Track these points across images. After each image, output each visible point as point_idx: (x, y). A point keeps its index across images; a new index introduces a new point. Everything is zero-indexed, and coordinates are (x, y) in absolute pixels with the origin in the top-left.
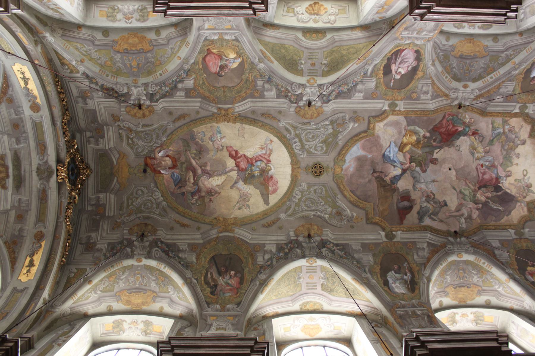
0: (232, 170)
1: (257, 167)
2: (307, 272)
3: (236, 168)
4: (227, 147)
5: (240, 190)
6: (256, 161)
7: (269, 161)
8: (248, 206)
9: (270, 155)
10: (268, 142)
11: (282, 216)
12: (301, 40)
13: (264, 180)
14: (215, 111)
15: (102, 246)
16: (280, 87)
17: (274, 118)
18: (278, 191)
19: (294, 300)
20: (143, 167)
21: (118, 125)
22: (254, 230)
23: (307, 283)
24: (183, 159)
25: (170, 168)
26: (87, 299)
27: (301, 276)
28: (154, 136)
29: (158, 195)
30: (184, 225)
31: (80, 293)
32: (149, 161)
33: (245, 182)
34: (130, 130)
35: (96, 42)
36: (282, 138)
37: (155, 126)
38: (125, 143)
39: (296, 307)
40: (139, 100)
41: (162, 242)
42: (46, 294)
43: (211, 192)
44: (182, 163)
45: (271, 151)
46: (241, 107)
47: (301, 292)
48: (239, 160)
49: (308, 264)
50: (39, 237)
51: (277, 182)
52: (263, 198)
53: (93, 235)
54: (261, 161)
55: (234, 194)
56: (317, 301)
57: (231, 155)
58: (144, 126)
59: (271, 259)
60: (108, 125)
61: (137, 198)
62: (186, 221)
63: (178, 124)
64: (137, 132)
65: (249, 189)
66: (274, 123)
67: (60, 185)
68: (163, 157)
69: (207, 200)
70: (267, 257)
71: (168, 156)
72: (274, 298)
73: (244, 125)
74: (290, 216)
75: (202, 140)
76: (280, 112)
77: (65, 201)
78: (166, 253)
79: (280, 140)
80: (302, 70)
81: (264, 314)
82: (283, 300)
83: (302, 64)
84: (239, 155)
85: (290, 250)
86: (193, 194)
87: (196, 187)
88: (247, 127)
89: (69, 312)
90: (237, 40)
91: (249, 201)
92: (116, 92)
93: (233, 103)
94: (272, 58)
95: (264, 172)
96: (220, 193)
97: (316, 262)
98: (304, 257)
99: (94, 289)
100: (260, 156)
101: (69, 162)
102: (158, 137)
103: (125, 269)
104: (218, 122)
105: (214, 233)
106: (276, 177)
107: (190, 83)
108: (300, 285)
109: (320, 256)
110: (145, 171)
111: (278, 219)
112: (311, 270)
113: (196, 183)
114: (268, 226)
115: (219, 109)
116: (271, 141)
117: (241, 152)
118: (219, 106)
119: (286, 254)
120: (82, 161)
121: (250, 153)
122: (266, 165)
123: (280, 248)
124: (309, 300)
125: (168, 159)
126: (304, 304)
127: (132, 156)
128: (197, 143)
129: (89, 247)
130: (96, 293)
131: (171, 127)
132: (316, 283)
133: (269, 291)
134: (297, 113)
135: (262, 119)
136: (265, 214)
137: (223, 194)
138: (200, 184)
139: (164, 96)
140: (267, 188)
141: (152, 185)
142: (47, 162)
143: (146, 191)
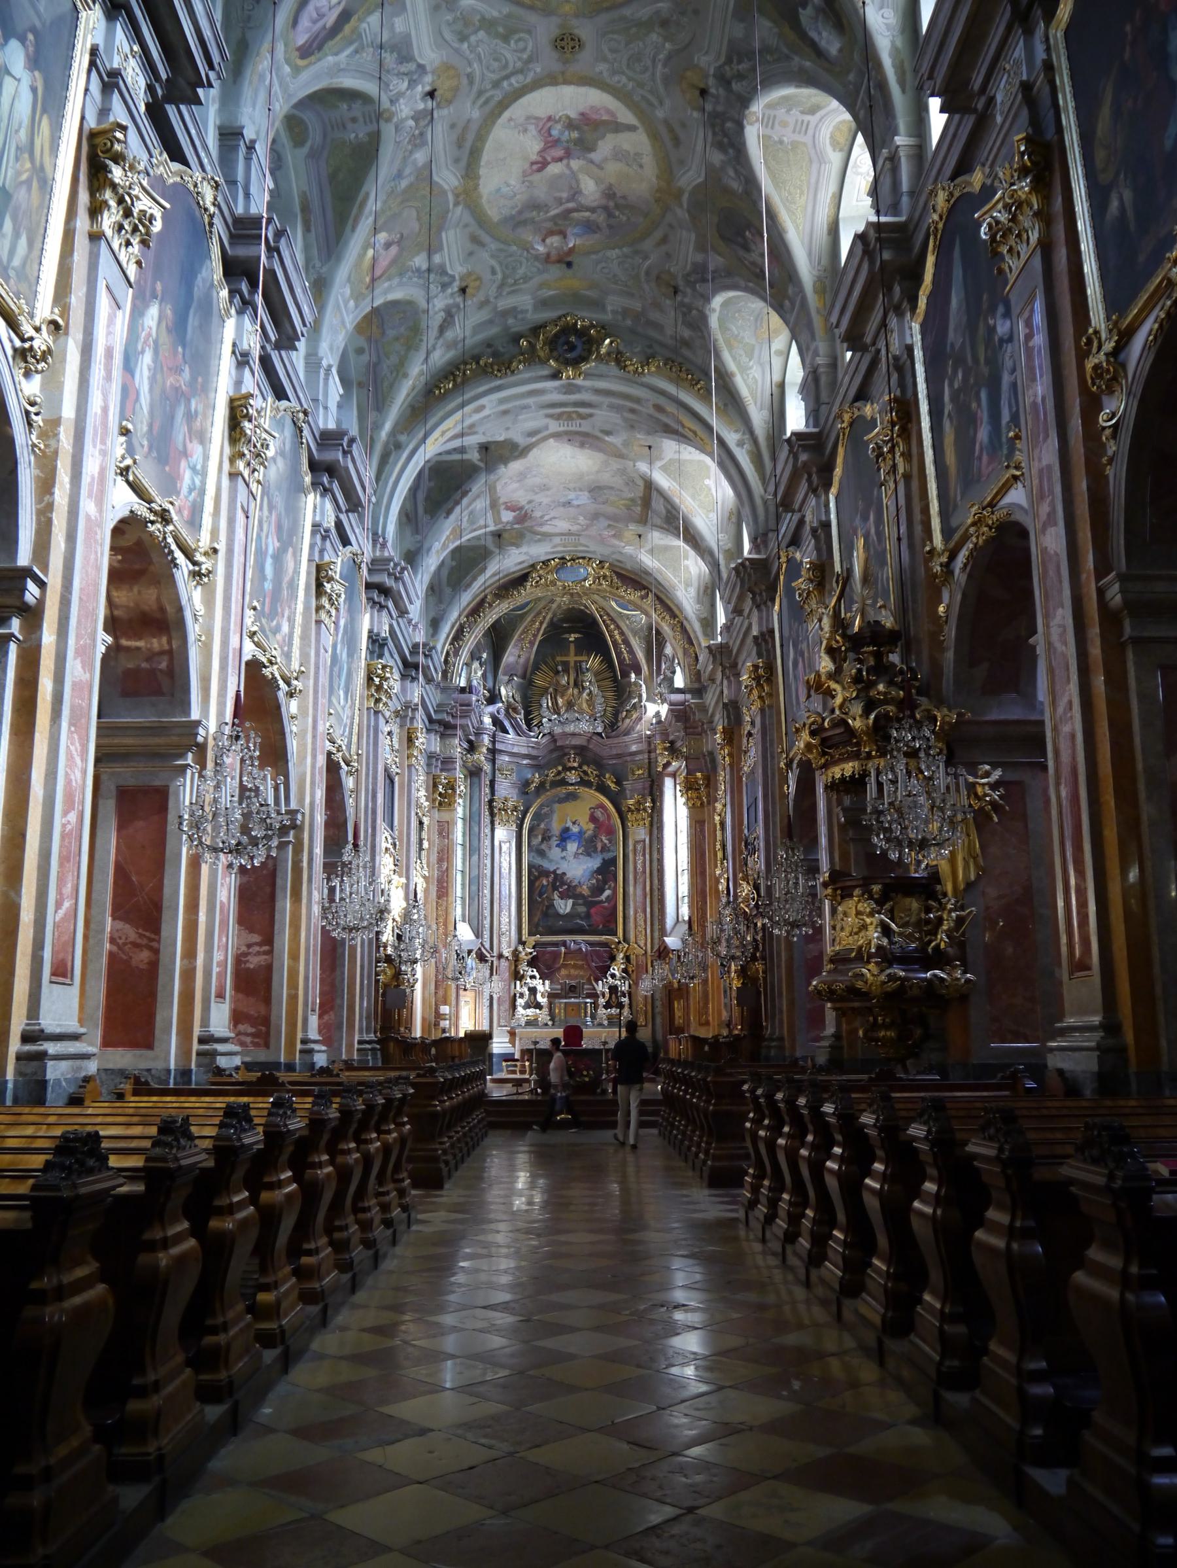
0: (568, 166)
1: (562, 133)
2: (772, 128)
3: (565, 162)
4: (524, 176)
5: (606, 160)
6: (550, 135)
7: (550, 118)
8: (636, 154)
9: (537, 118)
10: (512, 123)
11: (660, 114)
12: (311, 148)
13: (587, 125)
14: (460, 208)
15: (686, 333)
16: (407, 154)
17: (465, 128)
18: (611, 107)
19: (822, 160)
20: (564, 266)
21: (496, 298)
22: (682, 162)
23: (794, 132)
24: (549, 225)
25: (565, 237)
26: (756, 381)
27: (776, 139)
28: (510, 259)
29: (613, 253)
30: (664, 240)
31: (744, 391)
32: (554, 257)
33: (591, 149)
34: (502, 286)
35: (374, 359)
36: (504, 105)
37: (493, 262)
38: (523, 286)
39: (836, 158)
40: (452, 294)
41: (688, 275)
42: (732, 438)
43: (609, 193)
44: (556, 224)
45: (528, 118)
46: (448, 178)
47: (810, 143)
48: (549, 159)
49: (756, 125)
50: (659, 408)
51: (592, 107)
52: (622, 131)
53: (669, 331)
54: (550, 129)
55: (613, 168)
56: (833, 124)
57: (540, 170)
58: (494, 272)
59: (736, 171)
60: (496, 307)
61: (615, 276)
62: (658, 234)
63: (486, 238)
64: (505, 277)
65: (605, 147)
66: (474, 127)
67: (588, 376)
68: (545, 246)
69: (622, 201)
70: (731, 173)
71: (543, 240)
72: (804, 198)
73: (482, 163)
74: (661, 103)
75: (513, 208)
76: (453, 126)
77: (612, 369)
78: (704, 280)
79: (507, 107)
80: (369, 134)
81: (825, 226)
82: (813, 180)
83: (357, 136)
84: (540, 159)
85: (726, 135)
86: (610, 215)
87: (599, 211)
88: (486, 157)
89: (766, 414)
90: (349, 280)
91: (628, 152)
92: (445, 321)
93: (444, 192)
94: (360, 198)
95: (571, 125)
96: (611, 185)
97: (755, 113)
98: (740, 127)
99: (744, 369)
100: (540, 131)
101: (556, 360)
102: (511, 256)
103: (723, 327)
104: (480, 196)
105: (682, 214)
106: (581, 109)
107: (420, 261)
108: (795, 145)
109: (745, 102)
110: (569, 265)
111: (666, 122)
112: (769, 122)
113: (592, 210)
114: (677, 141)
115: (456, 204)
116: (510, 119)
117: (534, 157)
118: (451, 206)
119: (732, 145)
120: (555, 322)
121: (533, 145)
122: (557, 122)
123: (721, 147)
124: (828, 136)
125: (548, 241)
126: (835, 144)
127: (546, 276)
128: (520, 212)
129: (686, 343)
130: (751, 368)
131: (493, 246)
132: (797, 121)
133: (788, 210)
134: (449, 102)
135: (468, 145)
136: (654, 136)
137: (613, 181)
138: (595, 204)
139: (444, 272)
140: (604, 123)
141: (594, 257)
142: (556, 388)
143: (604, 264)
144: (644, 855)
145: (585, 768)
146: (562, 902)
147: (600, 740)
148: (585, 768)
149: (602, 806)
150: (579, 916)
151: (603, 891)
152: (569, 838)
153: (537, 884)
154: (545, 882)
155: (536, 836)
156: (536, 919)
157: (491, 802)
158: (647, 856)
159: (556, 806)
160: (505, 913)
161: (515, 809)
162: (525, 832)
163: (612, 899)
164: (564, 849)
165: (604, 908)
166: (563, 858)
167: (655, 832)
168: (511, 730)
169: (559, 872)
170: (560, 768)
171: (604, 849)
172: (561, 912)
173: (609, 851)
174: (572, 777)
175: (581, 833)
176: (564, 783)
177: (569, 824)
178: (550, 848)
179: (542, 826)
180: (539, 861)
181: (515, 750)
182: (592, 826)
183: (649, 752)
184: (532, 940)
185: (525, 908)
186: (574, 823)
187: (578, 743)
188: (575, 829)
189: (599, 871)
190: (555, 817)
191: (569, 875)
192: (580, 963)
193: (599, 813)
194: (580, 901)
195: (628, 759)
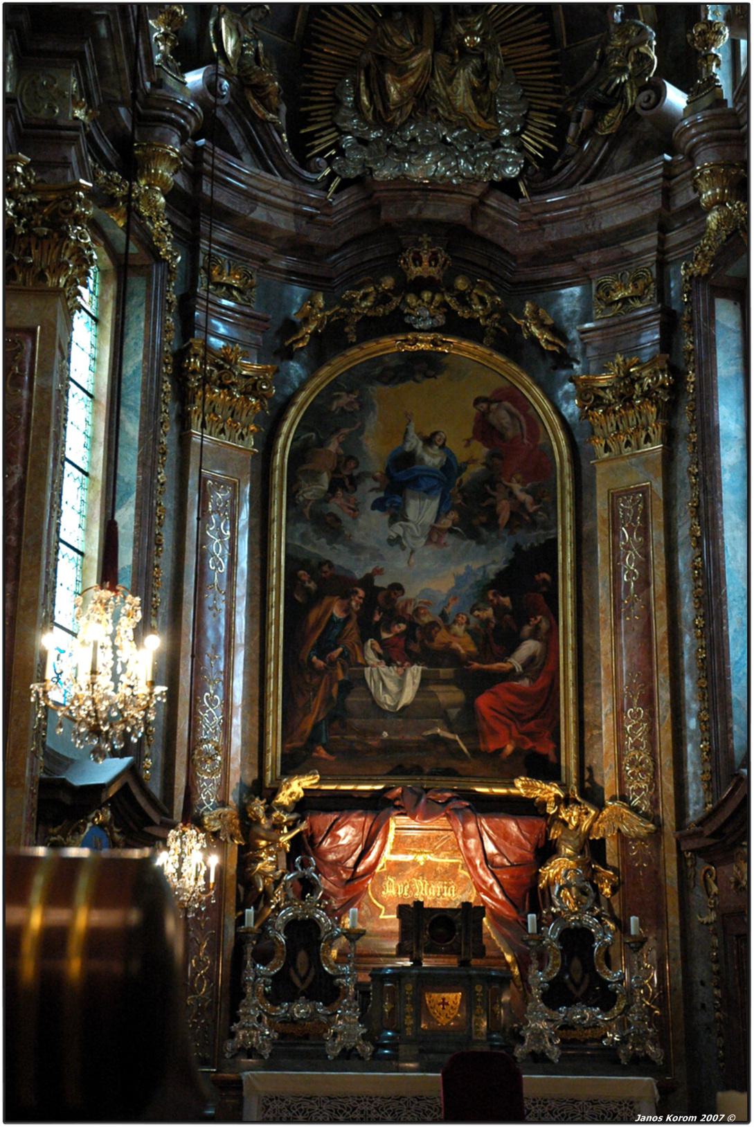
144: (644, 532)
145: (461, 284)
146: (389, 674)
147: (512, 207)
148: (461, 284)
149: (514, 396)
150: (441, 713)
151: (513, 644)
152: (414, 483)
153: (313, 616)
154: (337, 612)
155: (314, 476)
156: (308, 725)
157: (181, 356)
158: (657, 534)
159: (377, 391)
160: (213, 693)
161: (252, 388)
162: (280, 459)
163: (545, 665)
164: (398, 515)
165: (522, 694)
166: (396, 541)
167: (684, 456)
168: (246, 157)
169: (381, 582)
170: (388, 283)
171: (519, 517)
172: (387, 700)
173: (533, 525)
174: (423, 309)
175: (450, 468)
176: (397, 324)
177: (414, 443)
178: (355, 511)
179: (333, 446)
180: (320, 548)
181: (259, 214)
182: (480, 451)
183: (664, 229)
184: (297, 787)
185: (276, 687)
186: (428, 441)
187: (442, 215)
188: (432, 459)
189: (503, 582)
190: (373, 423)
191: (413, 592)
192: (444, 860)
193: (502, 416)
194: (446, 672)
195: (595, 257)
